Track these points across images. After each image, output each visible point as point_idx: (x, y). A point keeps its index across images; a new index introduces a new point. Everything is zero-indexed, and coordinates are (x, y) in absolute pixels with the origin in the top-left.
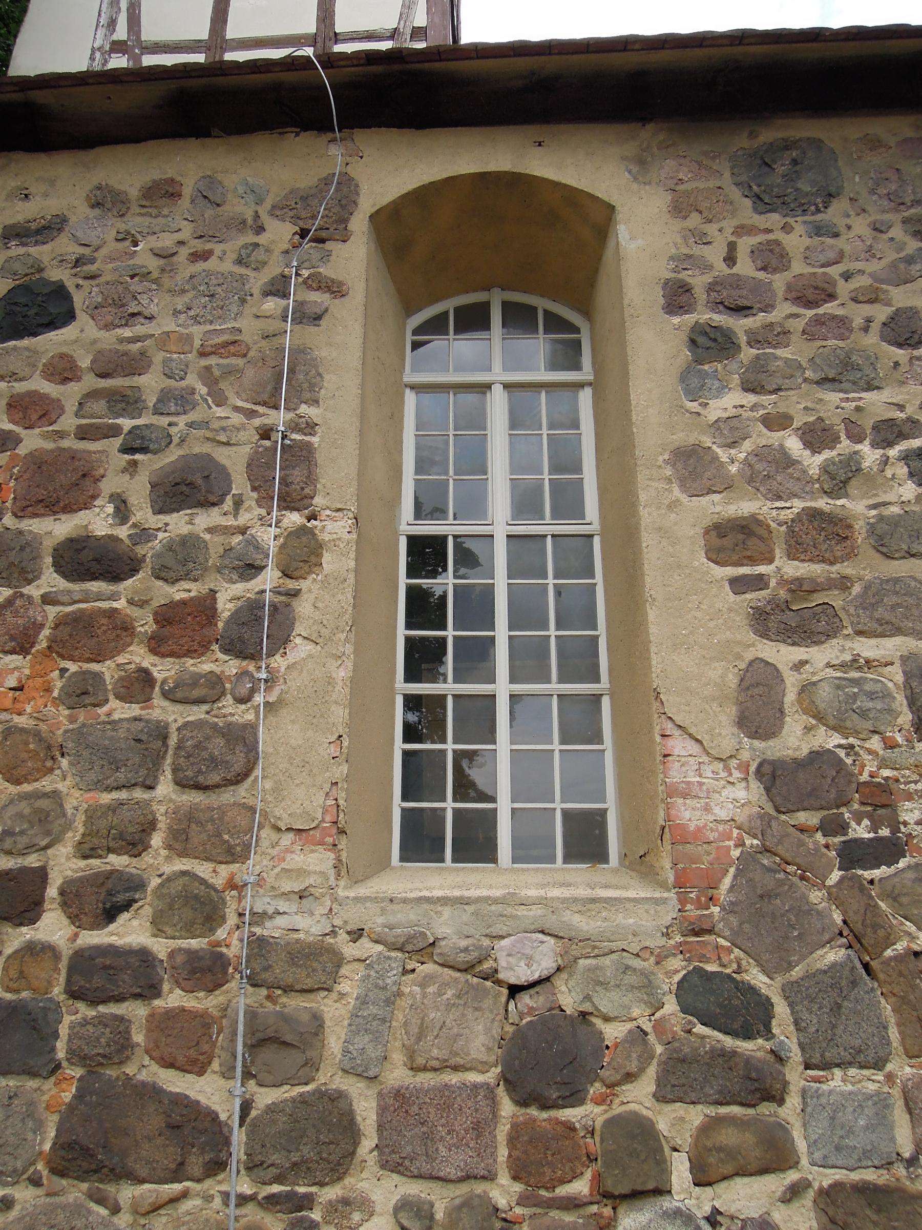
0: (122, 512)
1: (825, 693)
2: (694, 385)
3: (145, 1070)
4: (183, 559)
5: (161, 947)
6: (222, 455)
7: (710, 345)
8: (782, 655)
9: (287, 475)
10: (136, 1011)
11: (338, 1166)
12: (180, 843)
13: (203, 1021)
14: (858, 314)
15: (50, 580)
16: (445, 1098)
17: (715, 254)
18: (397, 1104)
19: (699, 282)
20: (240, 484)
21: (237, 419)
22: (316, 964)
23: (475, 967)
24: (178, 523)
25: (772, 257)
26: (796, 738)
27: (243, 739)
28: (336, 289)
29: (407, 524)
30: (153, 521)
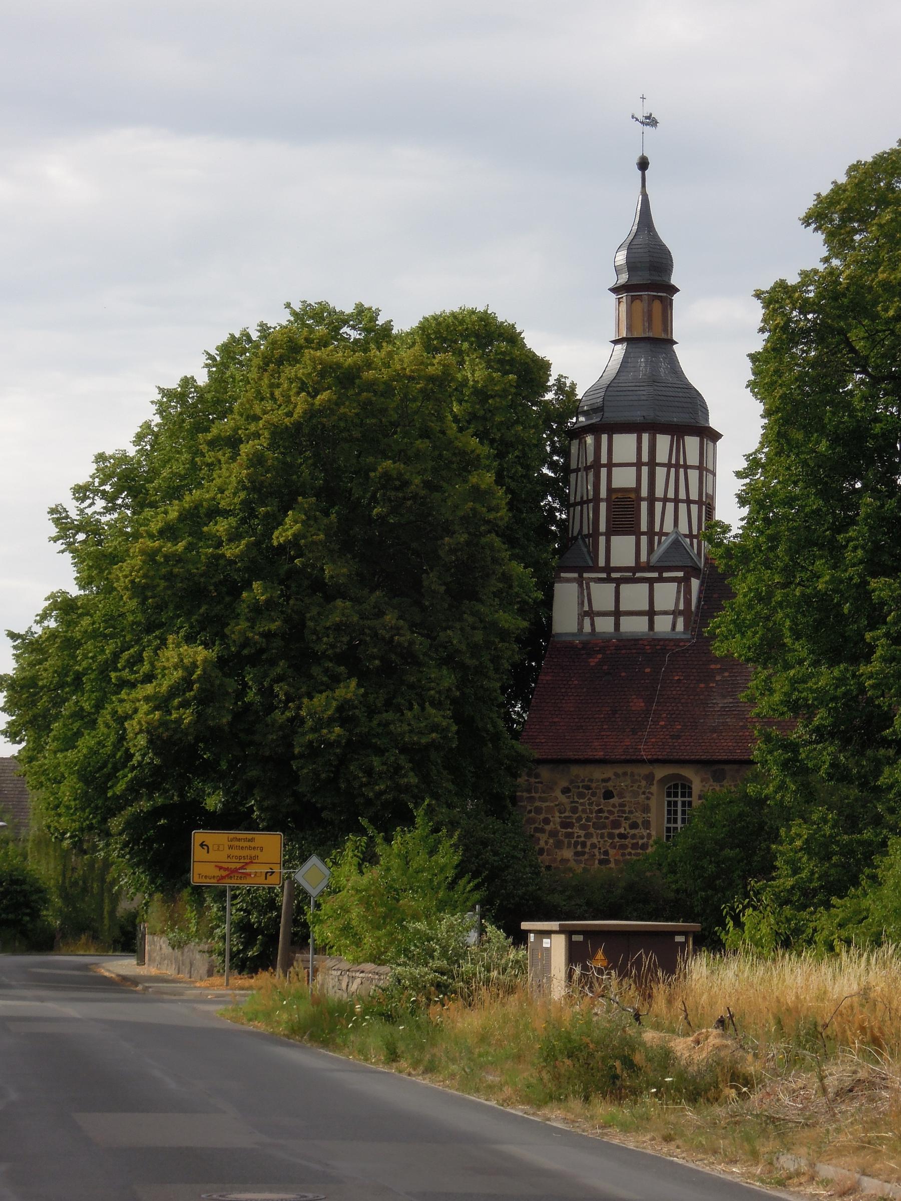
9: (647, 824)
15: (617, 839)
24: (633, 832)
28: (652, 794)
29: (666, 825)
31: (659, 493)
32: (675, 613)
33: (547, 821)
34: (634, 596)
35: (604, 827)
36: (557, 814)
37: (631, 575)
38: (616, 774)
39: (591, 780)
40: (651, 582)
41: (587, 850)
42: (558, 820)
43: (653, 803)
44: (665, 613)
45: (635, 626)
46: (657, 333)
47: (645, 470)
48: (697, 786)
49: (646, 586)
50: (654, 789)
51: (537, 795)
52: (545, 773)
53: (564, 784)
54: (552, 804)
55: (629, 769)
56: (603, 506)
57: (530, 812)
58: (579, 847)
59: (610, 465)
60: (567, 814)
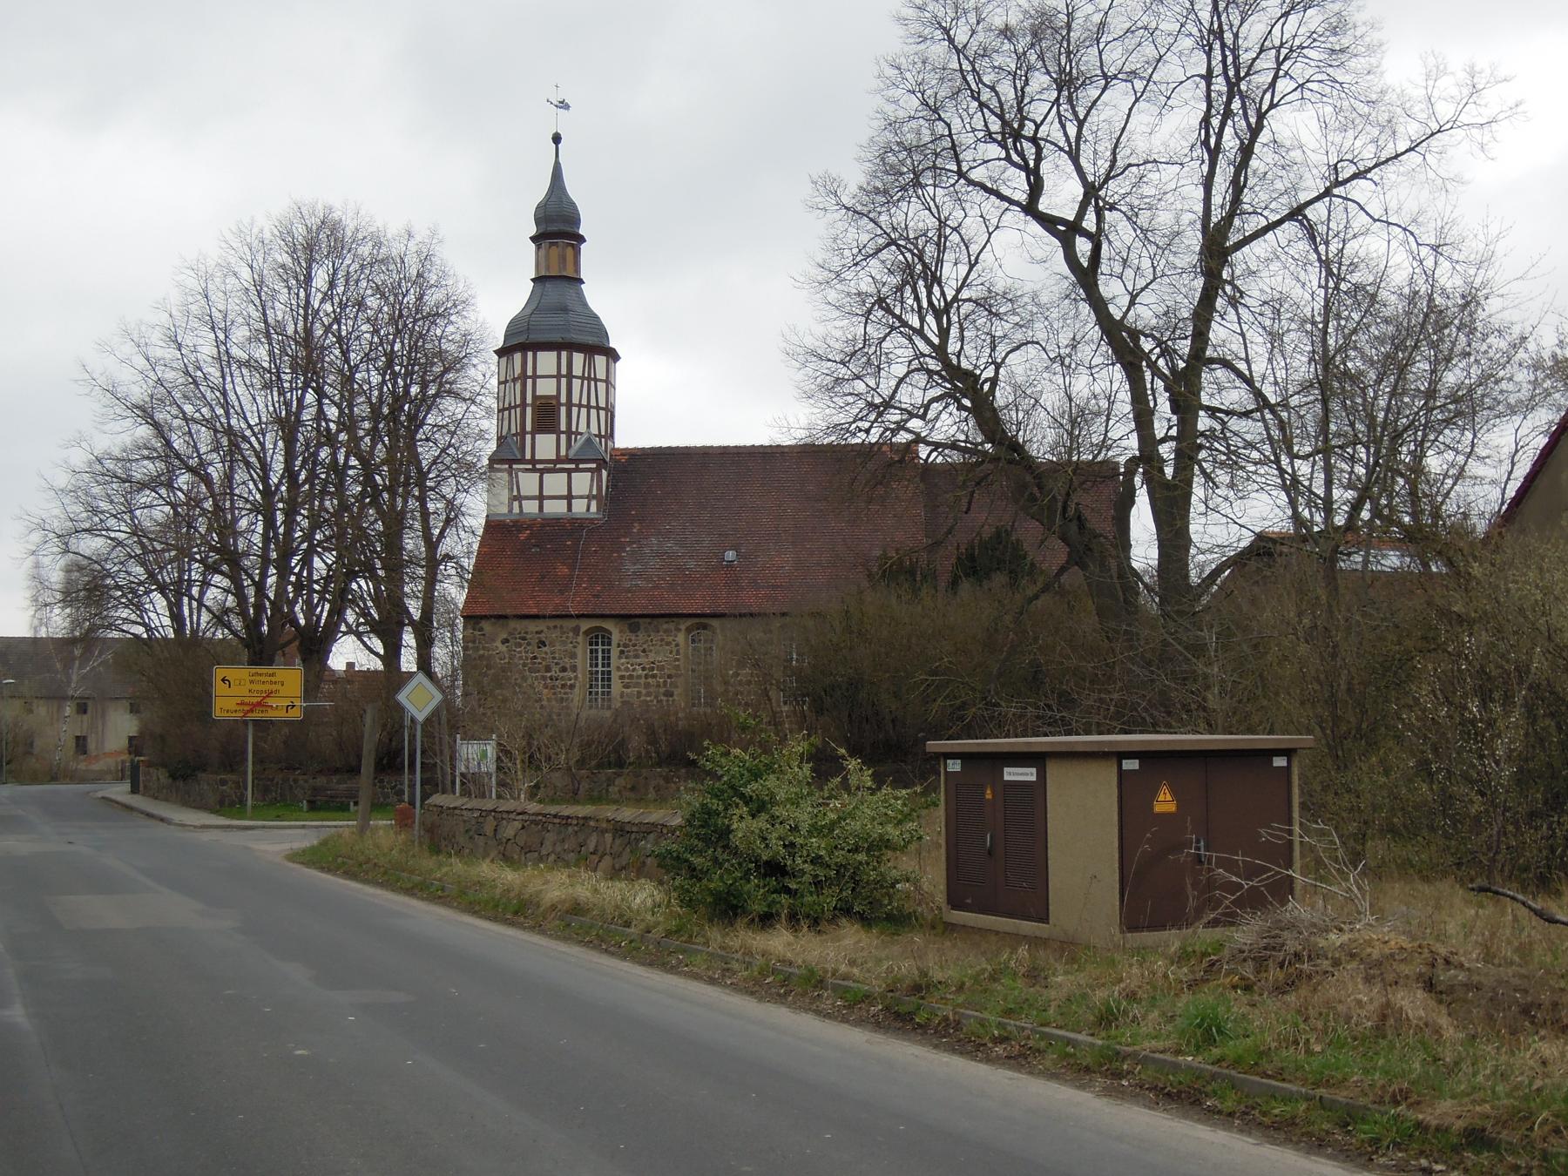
7: (622, 652)
9: (574, 668)
31: (575, 400)
32: (589, 497)
34: (555, 483)
37: (553, 466)
40: (569, 471)
43: (579, 651)
44: (581, 497)
45: (555, 508)
46: (570, 273)
47: (564, 381)
48: (615, 638)
49: (565, 475)
50: (580, 639)
55: (558, 622)
56: (529, 410)
59: (535, 377)
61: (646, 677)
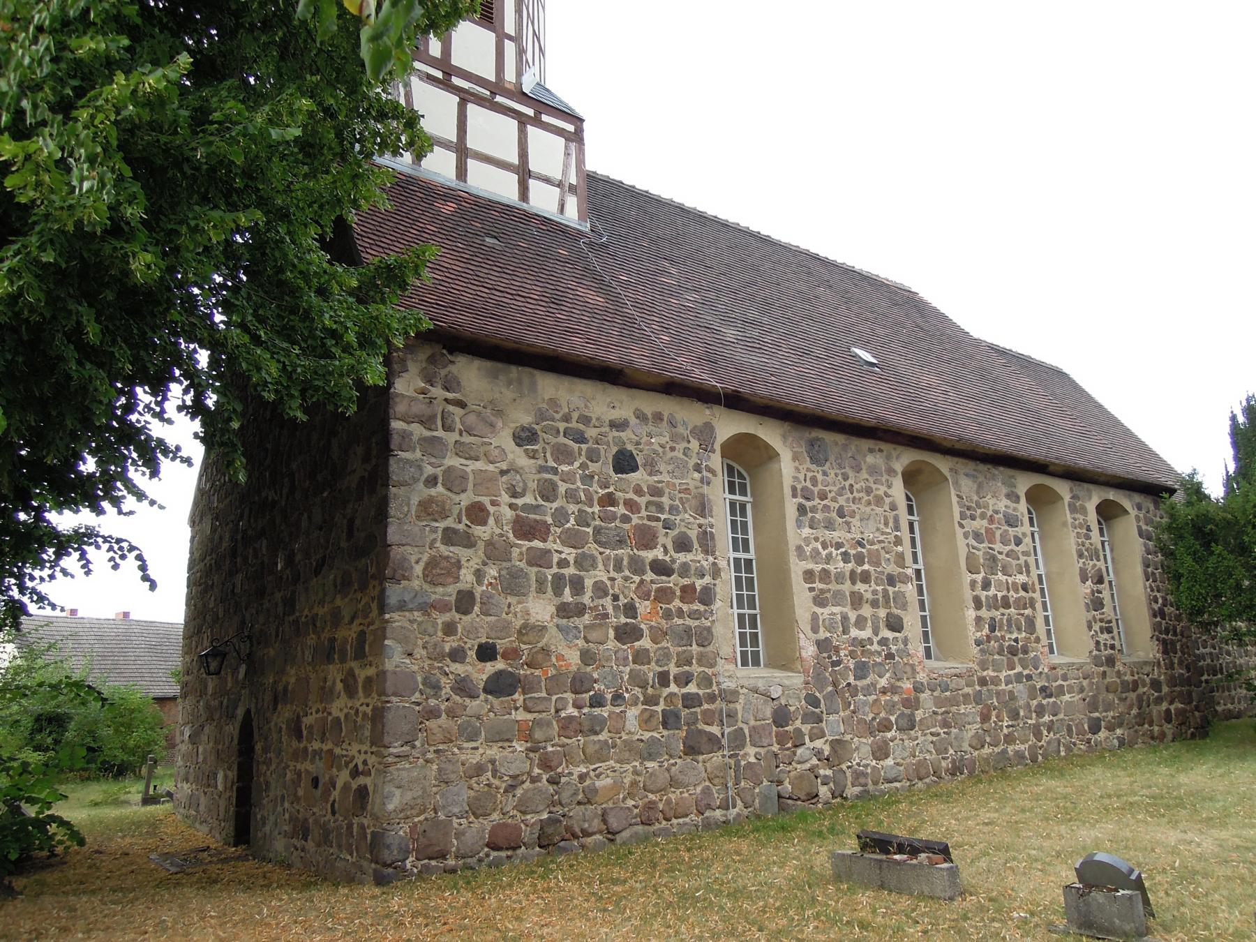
0: (666, 551)
1: (827, 622)
2: (799, 525)
3: (701, 726)
4: (685, 570)
5: (701, 692)
6: (689, 532)
7: (802, 510)
8: (819, 610)
9: (707, 542)
10: (698, 710)
11: (743, 746)
12: (700, 663)
13: (713, 712)
14: (833, 504)
15: (649, 576)
16: (763, 726)
17: (802, 477)
18: (753, 729)
19: (799, 487)
20: (696, 545)
21: (692, 520)
22: (735, 693)
23: (766, 695)
24: (682, 557)
25: (814, 481)
26: (823, 634)
27: (709, 629)
30: (676, 556)
33: (477, 514)
35: (621, 543)
36: (505, 498)
38: (641, 416)
39: (585, 420)
40: (523, 121)
41: (586, 599)
42: (509, 514)
45: (494, 184)
51: (451, 438)
52: (471, 375)
53: (526, 419)
54: (491, 467)
57: (432, 481)
58: (567, 591)
60: (528, 499)
61: (853, 577)
